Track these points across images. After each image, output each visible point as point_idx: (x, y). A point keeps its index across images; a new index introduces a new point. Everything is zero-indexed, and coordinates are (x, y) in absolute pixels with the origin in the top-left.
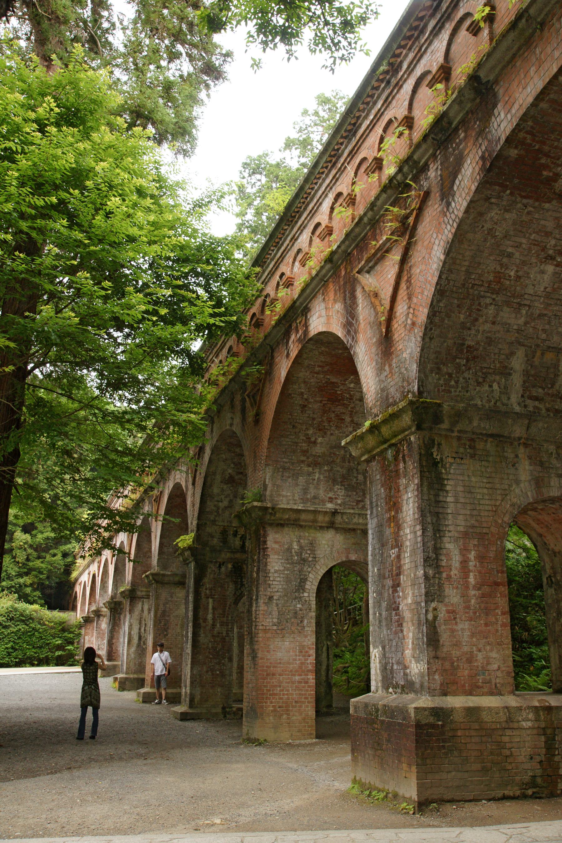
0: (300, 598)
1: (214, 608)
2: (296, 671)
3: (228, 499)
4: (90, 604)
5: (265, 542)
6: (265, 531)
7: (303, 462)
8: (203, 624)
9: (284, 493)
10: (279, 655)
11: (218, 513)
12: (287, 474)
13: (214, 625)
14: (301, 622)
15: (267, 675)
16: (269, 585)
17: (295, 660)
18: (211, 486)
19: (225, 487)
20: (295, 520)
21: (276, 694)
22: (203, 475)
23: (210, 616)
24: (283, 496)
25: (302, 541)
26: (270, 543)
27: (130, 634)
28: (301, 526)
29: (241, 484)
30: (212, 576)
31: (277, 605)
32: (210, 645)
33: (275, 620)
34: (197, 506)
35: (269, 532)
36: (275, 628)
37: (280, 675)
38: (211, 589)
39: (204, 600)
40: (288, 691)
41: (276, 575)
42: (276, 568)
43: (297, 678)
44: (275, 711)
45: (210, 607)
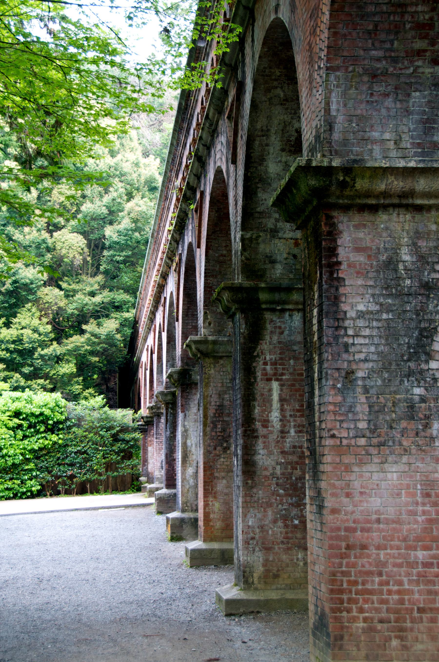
0: (421, 372)
1: (282, 400)
2: (418, 539)
5: (333, 251)
6: (333, 225)
7: (420, 53)
8: (262, 431)
9: (376, 135)
10: (375, 503)
12: (379, 88)
13: (283, 432)
14: (427, 426)
15: (348, 547)
16: (346, 346)
17: (413, 513)
18: (262, 159)
20: (404, 195)
21: (371, 592)
22: (245, 138)
23: (275, 415)
24: (374, 142)
25: (422, 243)
26: (345, 252)
27: (185, 445)
28: (419, 209)
30: (275, 338)
31: (366, 390)
32: (278, 471)
33: (362, 425)
34: (240, 203)
35: (341, 227)
36: (362, 441)
37: (378, 548)
38: (274, 364)
39: (260, 385)
40: (400, 583)
41: (361, 323)
42: (361, 307)
43: (421, 555)
44: (371, 630)
45: (275, 397)
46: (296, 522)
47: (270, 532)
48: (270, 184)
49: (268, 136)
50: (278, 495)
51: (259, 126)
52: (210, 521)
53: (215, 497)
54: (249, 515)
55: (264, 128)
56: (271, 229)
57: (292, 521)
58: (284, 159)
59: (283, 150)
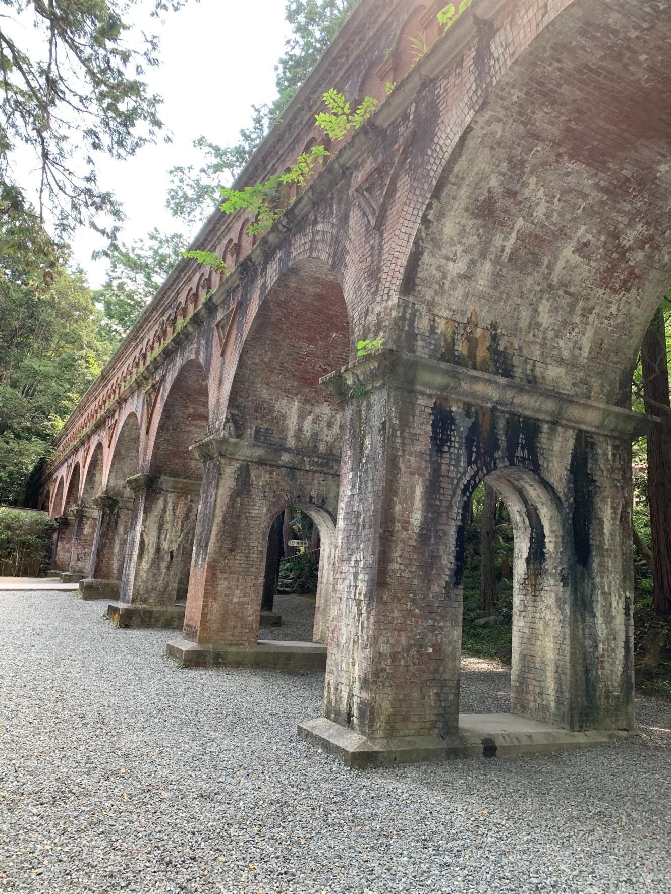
3: (467, 258)
4: (67, 503)
11: (442, 287)
18: (441, 215)
19: (470, 223)
29: (502, 224)
39: (403, 479)
46: (430, 650)
47: (403, 662)
48: (440, 248)
49: (459, 186)
50: (414, 616)
51: (456, 169)
52: (207, 621)
53: (215, 598)
54: (381, 641)
55: (460, 175)
56: (429, 301)
57: (426, 650)
58: (463, 222)
59: (467, 210)
